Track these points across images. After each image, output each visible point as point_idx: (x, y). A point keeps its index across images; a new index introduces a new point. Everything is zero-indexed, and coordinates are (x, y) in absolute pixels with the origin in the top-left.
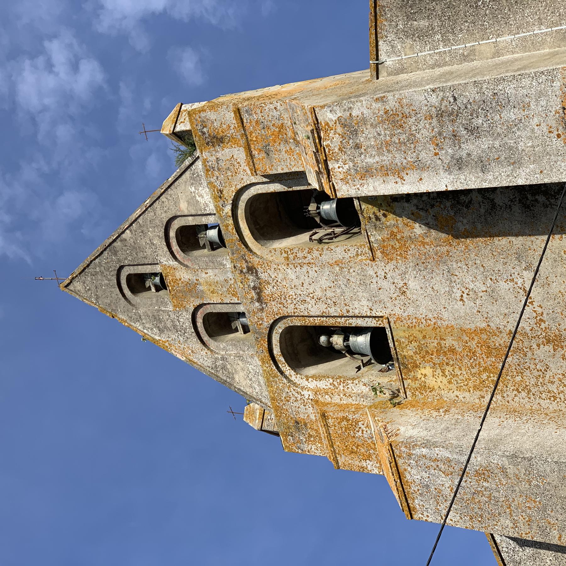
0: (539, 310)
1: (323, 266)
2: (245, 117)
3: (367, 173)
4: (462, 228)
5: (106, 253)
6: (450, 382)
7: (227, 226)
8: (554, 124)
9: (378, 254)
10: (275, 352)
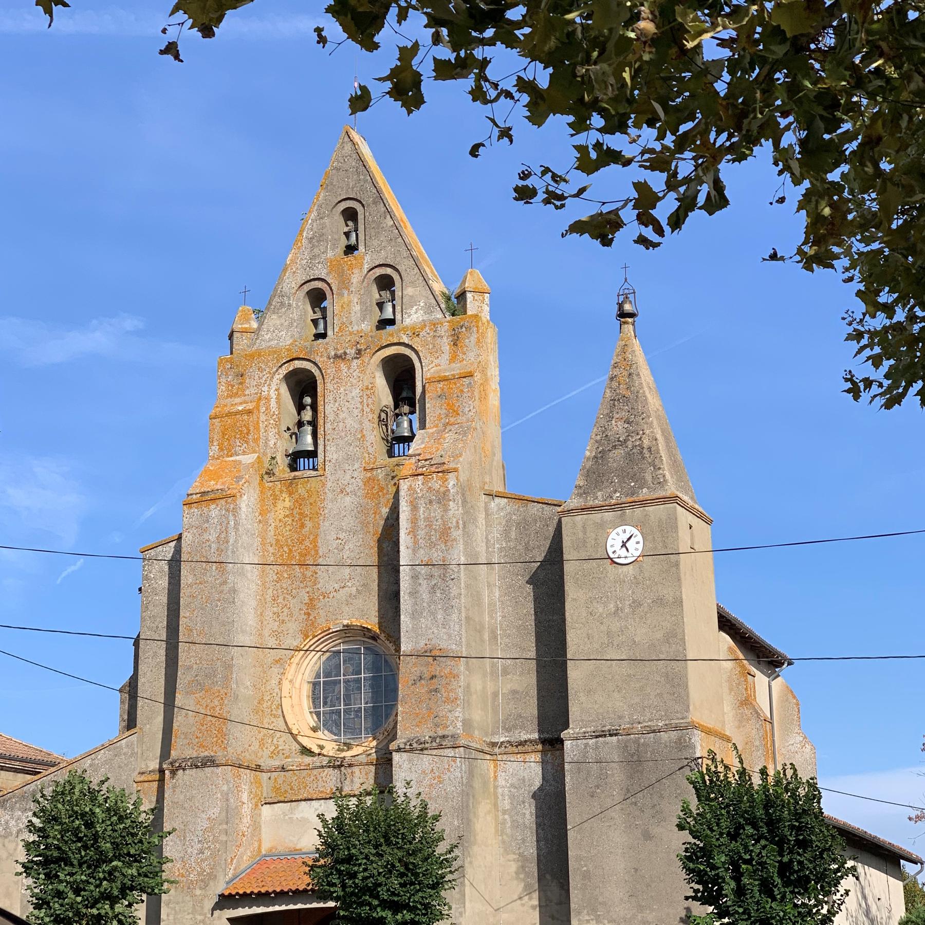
0: (331, 596)
1: (361, 423)
2: (467, 381)
3: (414, 508)
4: (385, 545)
5: (374, 191)
6: (280, 520)
7: (392, 335)
8: (433, 642)
9: (369, 475)
10: (296, 362)
